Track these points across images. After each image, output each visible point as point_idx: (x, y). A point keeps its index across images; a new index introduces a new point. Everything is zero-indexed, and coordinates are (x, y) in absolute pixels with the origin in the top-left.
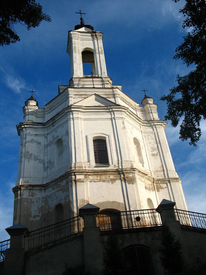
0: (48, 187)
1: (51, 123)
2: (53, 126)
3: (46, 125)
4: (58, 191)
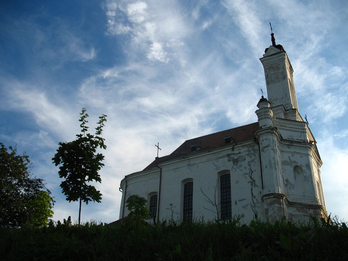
0: (293, 206)
1: (288, 143)
2: (289, 148)
4: (305, 215)
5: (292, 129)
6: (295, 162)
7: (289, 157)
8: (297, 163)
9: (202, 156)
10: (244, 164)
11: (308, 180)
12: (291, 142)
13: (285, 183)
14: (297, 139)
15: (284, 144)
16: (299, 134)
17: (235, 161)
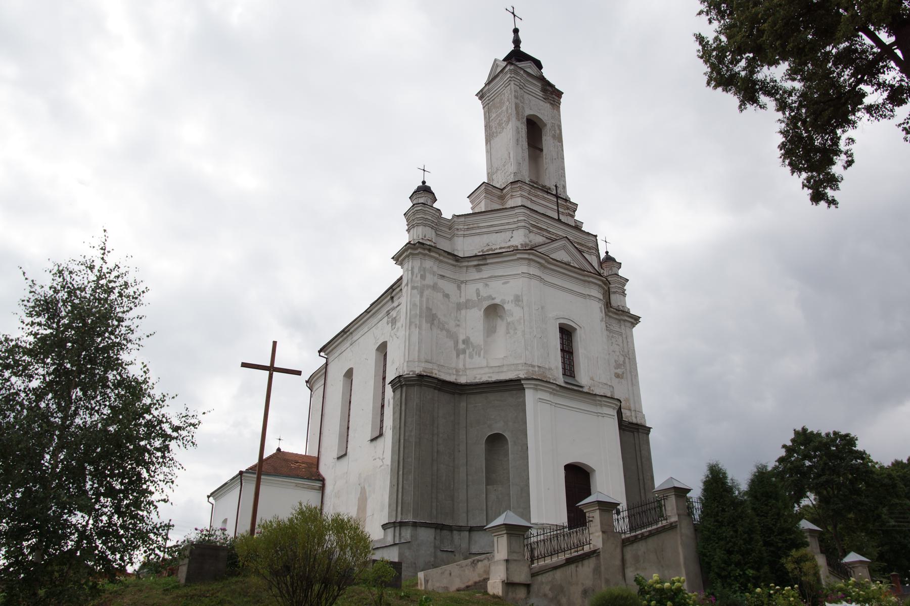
1: (475, 263)
2: (479, 271)
3: (462, 262)
5: (492, 229)
6: (490, 297)
7: (478, 289)
8: (493, 299)
9: (362, 324)
11: (516, 329)
12: (480, 258)
13: (461, 346)
14: (500, 248)
15: (467, 267)
16: (508, 234)
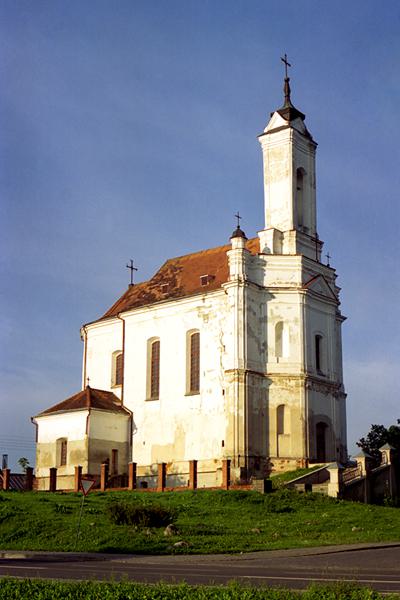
6: (279, 317)
10: (213, 321)
13: (262, 347)
17: (206, 317)
